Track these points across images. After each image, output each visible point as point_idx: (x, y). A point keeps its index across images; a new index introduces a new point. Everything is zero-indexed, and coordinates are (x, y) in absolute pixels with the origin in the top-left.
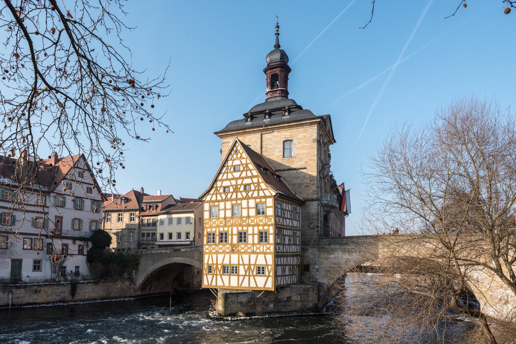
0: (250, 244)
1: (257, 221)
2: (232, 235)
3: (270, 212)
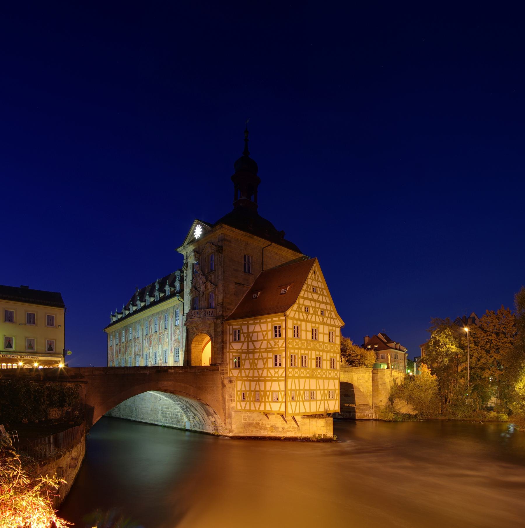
0: (324, 370)
1: (329, 348)
2: (311, 359)
3: (338, 340)
